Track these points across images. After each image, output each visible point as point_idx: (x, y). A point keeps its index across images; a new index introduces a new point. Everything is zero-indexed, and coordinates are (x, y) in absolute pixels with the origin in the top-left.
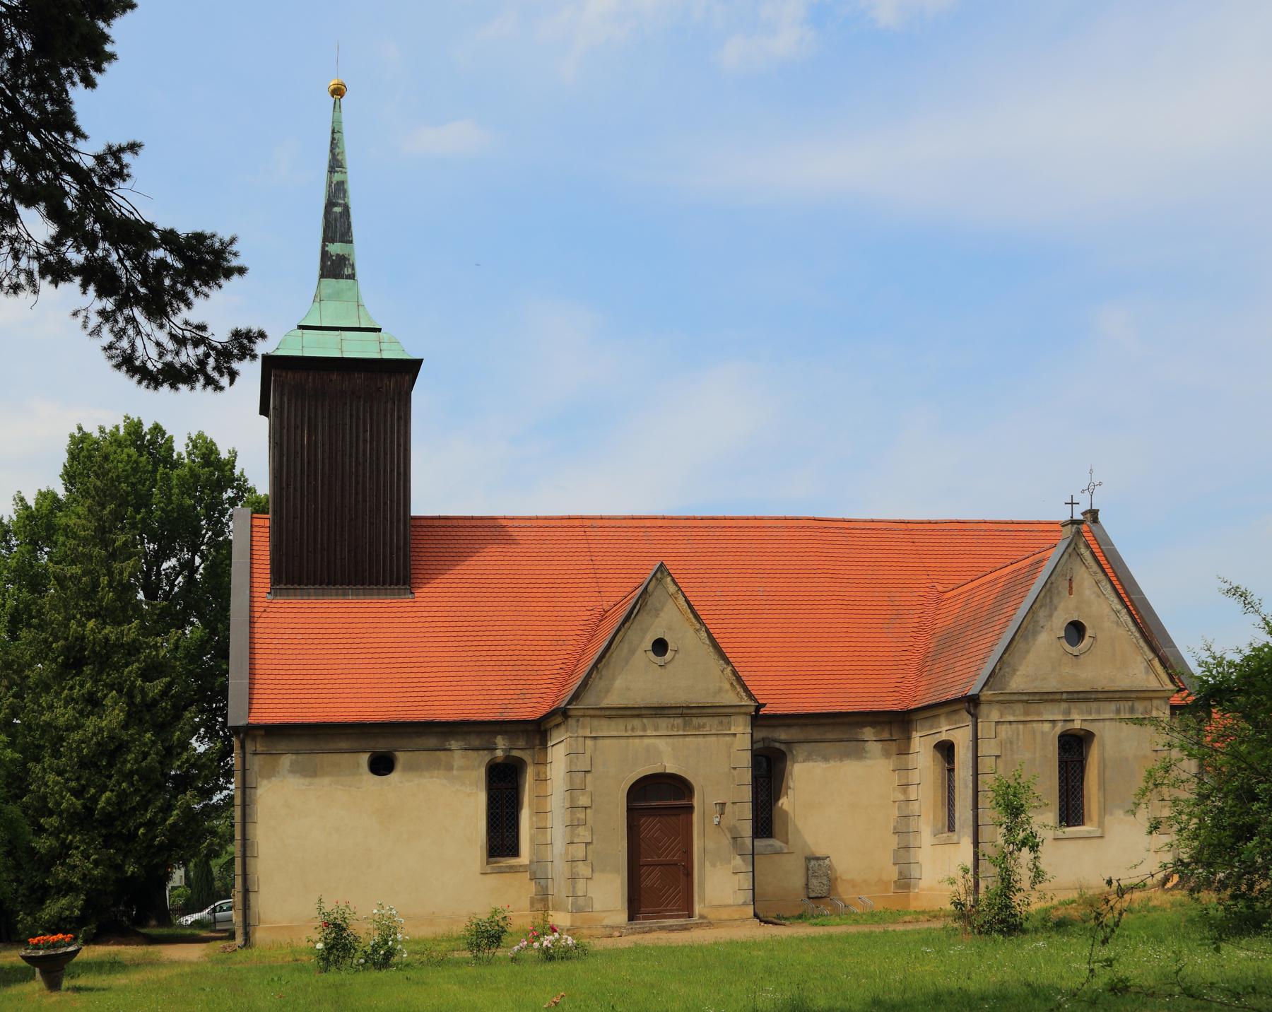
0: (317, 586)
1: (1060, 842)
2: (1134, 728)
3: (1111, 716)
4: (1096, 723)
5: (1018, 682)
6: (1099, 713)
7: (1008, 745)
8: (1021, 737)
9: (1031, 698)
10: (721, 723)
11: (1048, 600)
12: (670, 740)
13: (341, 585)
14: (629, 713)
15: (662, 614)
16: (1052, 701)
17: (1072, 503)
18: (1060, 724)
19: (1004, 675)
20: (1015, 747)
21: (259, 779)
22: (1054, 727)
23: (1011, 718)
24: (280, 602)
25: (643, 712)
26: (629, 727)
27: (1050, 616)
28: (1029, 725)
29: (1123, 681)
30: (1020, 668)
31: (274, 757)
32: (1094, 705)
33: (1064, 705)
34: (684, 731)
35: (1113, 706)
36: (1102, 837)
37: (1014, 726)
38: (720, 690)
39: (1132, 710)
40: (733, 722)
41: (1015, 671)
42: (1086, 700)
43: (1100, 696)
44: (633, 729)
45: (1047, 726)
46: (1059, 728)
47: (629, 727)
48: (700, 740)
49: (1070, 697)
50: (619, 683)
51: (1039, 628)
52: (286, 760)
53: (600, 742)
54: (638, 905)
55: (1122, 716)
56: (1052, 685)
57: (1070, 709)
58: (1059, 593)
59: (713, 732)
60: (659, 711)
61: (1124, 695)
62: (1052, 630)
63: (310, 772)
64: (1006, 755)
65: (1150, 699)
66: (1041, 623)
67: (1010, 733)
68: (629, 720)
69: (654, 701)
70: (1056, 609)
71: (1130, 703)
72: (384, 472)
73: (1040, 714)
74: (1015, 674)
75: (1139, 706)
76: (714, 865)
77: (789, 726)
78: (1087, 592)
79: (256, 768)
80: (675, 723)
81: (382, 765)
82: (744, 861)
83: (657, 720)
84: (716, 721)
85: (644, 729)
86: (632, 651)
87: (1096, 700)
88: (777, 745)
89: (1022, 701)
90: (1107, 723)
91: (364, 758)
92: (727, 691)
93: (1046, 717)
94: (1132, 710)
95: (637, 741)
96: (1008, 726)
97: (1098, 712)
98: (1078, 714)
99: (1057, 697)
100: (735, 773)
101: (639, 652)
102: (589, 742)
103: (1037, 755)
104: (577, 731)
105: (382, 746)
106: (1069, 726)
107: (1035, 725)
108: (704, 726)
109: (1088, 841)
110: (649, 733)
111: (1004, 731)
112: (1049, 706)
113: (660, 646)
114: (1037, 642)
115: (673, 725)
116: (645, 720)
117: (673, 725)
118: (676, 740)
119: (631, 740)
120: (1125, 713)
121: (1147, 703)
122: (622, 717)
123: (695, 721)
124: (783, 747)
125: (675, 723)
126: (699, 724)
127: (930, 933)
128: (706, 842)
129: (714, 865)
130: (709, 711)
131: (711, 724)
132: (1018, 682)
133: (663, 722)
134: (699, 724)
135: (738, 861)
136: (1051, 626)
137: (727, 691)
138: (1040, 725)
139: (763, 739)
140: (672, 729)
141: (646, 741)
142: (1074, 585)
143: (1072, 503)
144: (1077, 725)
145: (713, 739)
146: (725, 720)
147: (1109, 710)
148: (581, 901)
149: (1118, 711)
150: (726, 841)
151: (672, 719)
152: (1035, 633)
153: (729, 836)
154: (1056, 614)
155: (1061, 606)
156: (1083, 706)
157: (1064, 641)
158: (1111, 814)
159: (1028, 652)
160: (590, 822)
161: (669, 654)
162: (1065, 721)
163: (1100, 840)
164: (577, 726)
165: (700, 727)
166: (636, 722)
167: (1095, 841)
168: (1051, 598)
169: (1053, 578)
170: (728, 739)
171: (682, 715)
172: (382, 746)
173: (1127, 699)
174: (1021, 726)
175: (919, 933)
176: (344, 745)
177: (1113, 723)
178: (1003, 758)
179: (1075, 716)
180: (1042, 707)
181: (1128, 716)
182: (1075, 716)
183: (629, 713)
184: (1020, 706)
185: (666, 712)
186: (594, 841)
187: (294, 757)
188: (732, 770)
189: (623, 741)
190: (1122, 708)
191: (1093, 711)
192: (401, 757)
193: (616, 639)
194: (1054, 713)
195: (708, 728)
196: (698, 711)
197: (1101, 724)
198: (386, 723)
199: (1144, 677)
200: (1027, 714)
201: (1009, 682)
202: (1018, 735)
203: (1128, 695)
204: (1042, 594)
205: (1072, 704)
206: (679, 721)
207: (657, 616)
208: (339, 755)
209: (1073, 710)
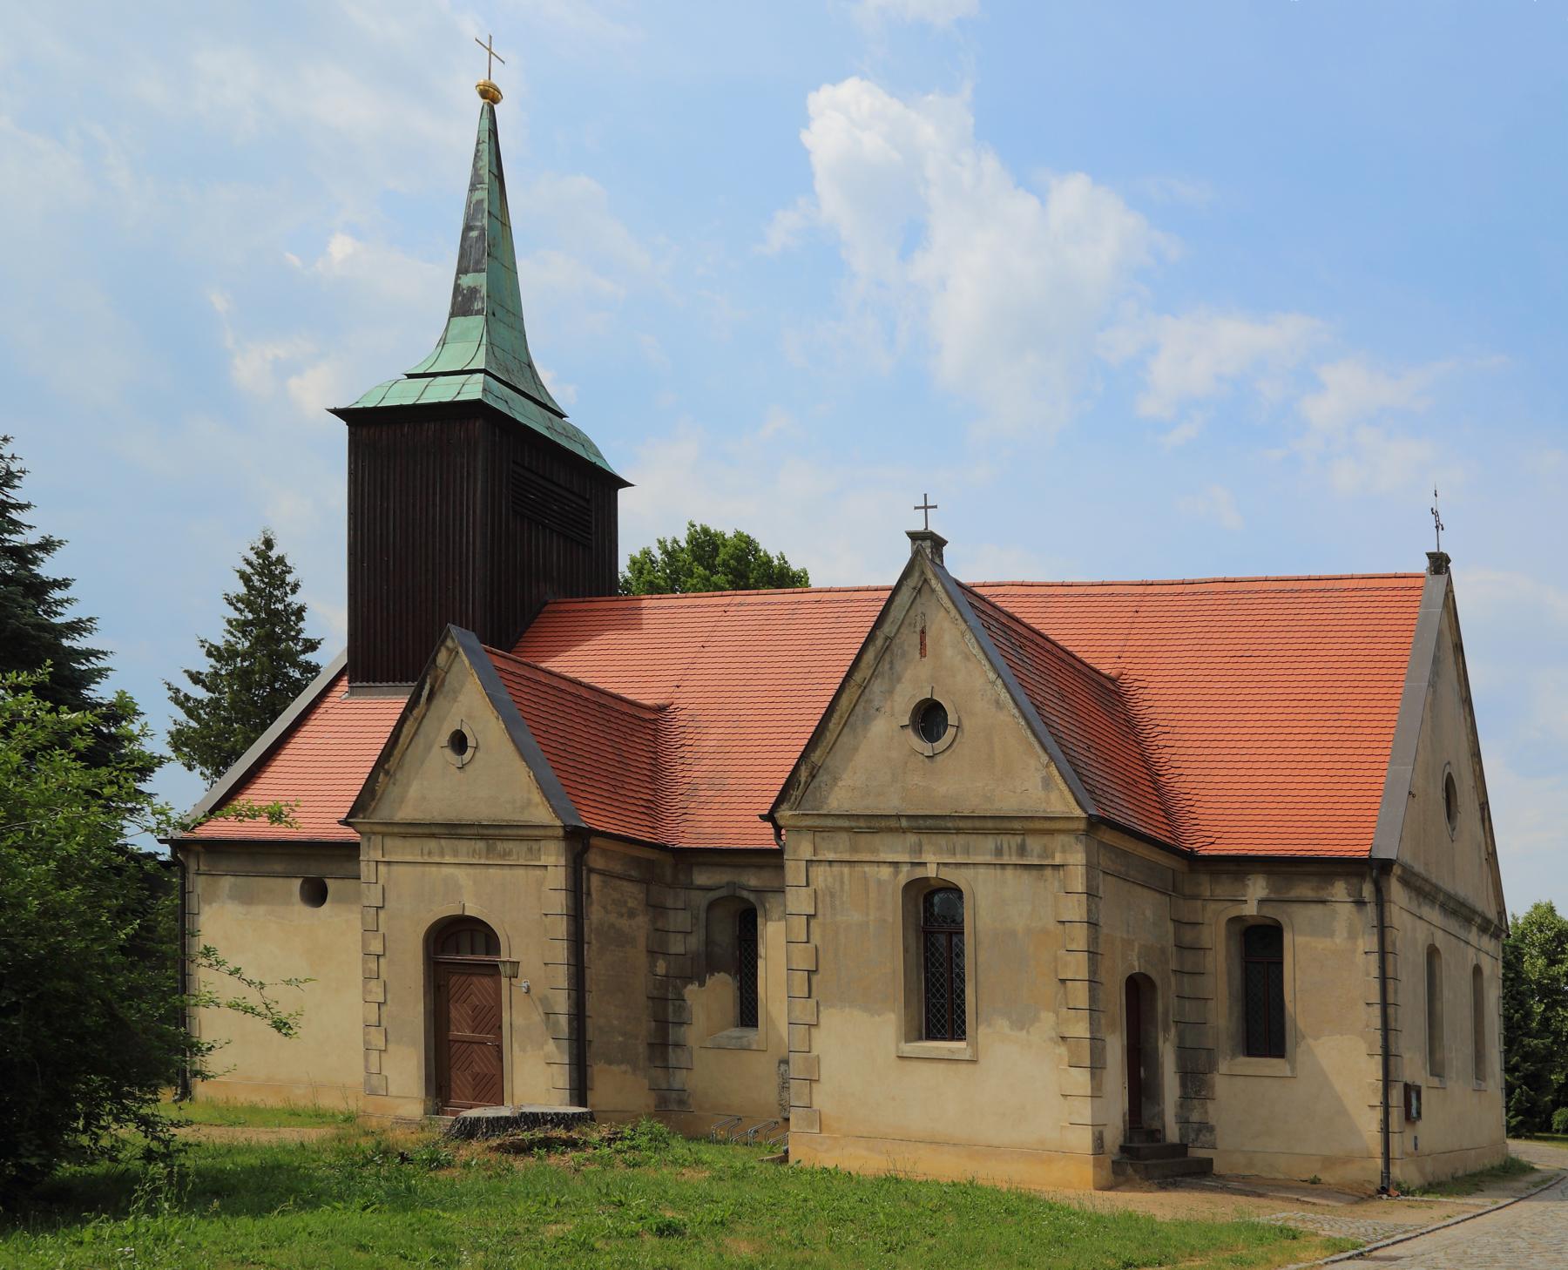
0: (391, 684)
1: (907, 1063)
2: (1026, 877)
3: (989, 859)
4: (964, 872)
5: (841, 797)
6: (968, 853)
7: (828, 898)
8: (846, 887)
9: (853, 824)
10: (530, 850)
11: (887, 666)
12: (471, 871)
13: (400, 682)
14: (419, 830)
15: (461, 698)
16: (890, 830)
17: (926, 507)
18: (905, 869)
19: (820, 787)
20: (837, 903)
21: (202, 904)
22: (896, 874)
23: (831, 856)
24: (354, 699)
25: (436, 830)
26: (426, 851)
27: (891, 692)
28: (858, 868)
29: (1007, 802)
30: (844, 776)
31: (216, 878)
32: (960, 840)
33: (912, 839)
34: (487, 858)
35: (990, 842)
36: (973, 1062)
37: (836, 869)
38: (529, 803)
39: (1022, 850)
40: (542, 849)
41: (835, 779)
42: (944, 831)
43: (961, 824)
44: (430, 853)
45: (886, 872)
46: (904, 876)
47: (426, 851)
48: (506, 871)
49: (914, 824)
50: (414, 791)
51: (872, 711)
52: (226, 882)
53: (395, 868)
54: (440, 1088)
55: (1006, 860)
56: (892, 803)
57: (920, 845)
58: (904, 654)
59: (522, 862)
60: (453, 830)
61: (999, 824)
62: (892, 715)
63: (247, 899)
64: (824, 915)
65: (1051, 832)
66: (876, 704)
67: (830, 879)
68: (425, 840)
69: (451, 815)
70: (899, 680)
71: (1019, 839)
72: (454, 542)
73: (875, 851)
74: (836, 785)
75: (1034, 844)
76: (523, 1050)
77: (761, 867)
78: (949, 652)
79: (199, 890)
80: (477, 847)
81: (316, 894)
82: (558, 1047)
83: (456, 842)
84: (524, 846)
85: (442, 854)
86: (429, 748)
87: (959, 831)
88: (745, 894)
89: (849, 830)
90: (982, 870)
91: (296, 884)
92: (537, 805)
93: (884, 857)
94: (1022, 850)
95: (434, 869)
96: (828, 868)
97: (967, 852)
98: (934, 854)
99: (893, 823)
100: (548, 920)
101: (436, 749)
102: (382, 868)
103: (872, 918)
104: (368, 854)
105: (314, 870)
106: (919, 873)
107: (867, 868)
108: (510, 853)
109: (953, 1067)
110: (447, 859)
111: (821, 875)
112: (888, 839)
113: (459, 742)
114: (869, 735)
115: (474, 850)
116: (443, 842)
117: (474, 850)
118: (478, 871)
119: (427, 869)
120: (1010, 855)
121: (1046, 839)
122: (416, 836)
123: (500, 846)
124: (752, 897)
125: (477, 847)
126: (504, 850)
127: (842, 1197)
128: (514, 1016)
129: (523, 1050)
130: (508, 832)
131: (518, 850)
132: (841, 797)
133: (464, 846)
134: (504, 850)
135: (551, 1046)
136: (892, 708)
137: (537, 805)
138: (875, 868)
139: (728, 883)
140: (473, 857)
141: (446, 870)
142: (928, 641)
143: (926, 507)
144: (931, 872)
145: (521, 871)
146: (535, 846)
147: (983, 850)
148: (375, 1080)
149: (999, 852)
150: (537, 1017)
151: (473, 842)
152: (867, 720)
153: (540, 1010)
154: (899, 688)
155: (908, 675)
156: (942, 840)
157: (910, 731)
158: (989, 1025)
159: (856, 749)
160: (383, 975)
161: (470, 752)
162: (913, 864)
163: (971, 1067)
164: (369, 846)
165: (505, 854)
166: (432, 844)
167: (963, 1067)
168: (891, 663)
169: (888, 629)
170: (538, 872)
171: (482, 838)
172: (314, 870)
173: (1012, 832)
174: (846, 870)
175: (1051, 1209)
176: (278, 867)
177: (992, 871)
178: (820, 917)
179: (929, 857)
180: (877, 839)
181: (1015, 860)
182: (929, 857)
183: (419, 830)
184: (844, 836)
185: (460, 831)
186: (389, 1002)
187: (232, 879)
188: (544, 917)
189: (419, 869)
190: (1005, 846)
191: (958, 849)
192: (331, 884)
193: (405, 731)
194: (895, 850)
195: (515, 857)
196: (497, 832)
197: (970, 872)
198: (331, 843)
199: (1041, 794)
200: (854, 849)
201: (826, 798)
202: (842, 883)
203: (942, 823)
204: (870, 656)
205: (924, 838)
206: (481, 845)
207: (455, 700)
208: (273, 879)
209: (925, 848)
